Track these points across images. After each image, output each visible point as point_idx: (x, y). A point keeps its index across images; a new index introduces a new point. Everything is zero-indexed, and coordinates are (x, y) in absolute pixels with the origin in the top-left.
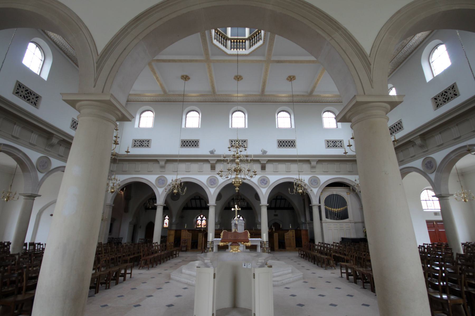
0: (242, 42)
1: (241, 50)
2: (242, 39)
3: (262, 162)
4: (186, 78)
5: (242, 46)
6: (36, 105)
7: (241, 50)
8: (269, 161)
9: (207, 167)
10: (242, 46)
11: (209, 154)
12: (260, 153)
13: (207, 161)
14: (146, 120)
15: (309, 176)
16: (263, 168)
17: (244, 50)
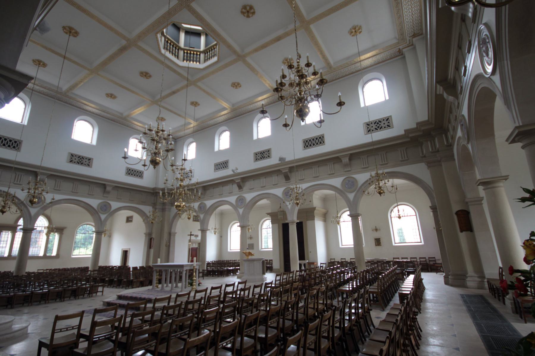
0: (197, 54)
1: (195, 63)
2: (197, 51)
3: (283, 171)
4: (195, 104)
5: (197, 58)
6: (89, 165)
7: (195, 63)
8: (291, 169)
9: (235, 186)
10: (197, 58)
11: (232, 173)
12: (277, 161)
13: (232, 182)
14: (191, 151)
15: (341, 179)
16: (287, 178)
17: (198, 63)
